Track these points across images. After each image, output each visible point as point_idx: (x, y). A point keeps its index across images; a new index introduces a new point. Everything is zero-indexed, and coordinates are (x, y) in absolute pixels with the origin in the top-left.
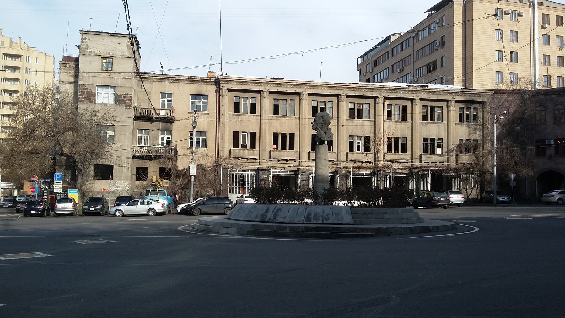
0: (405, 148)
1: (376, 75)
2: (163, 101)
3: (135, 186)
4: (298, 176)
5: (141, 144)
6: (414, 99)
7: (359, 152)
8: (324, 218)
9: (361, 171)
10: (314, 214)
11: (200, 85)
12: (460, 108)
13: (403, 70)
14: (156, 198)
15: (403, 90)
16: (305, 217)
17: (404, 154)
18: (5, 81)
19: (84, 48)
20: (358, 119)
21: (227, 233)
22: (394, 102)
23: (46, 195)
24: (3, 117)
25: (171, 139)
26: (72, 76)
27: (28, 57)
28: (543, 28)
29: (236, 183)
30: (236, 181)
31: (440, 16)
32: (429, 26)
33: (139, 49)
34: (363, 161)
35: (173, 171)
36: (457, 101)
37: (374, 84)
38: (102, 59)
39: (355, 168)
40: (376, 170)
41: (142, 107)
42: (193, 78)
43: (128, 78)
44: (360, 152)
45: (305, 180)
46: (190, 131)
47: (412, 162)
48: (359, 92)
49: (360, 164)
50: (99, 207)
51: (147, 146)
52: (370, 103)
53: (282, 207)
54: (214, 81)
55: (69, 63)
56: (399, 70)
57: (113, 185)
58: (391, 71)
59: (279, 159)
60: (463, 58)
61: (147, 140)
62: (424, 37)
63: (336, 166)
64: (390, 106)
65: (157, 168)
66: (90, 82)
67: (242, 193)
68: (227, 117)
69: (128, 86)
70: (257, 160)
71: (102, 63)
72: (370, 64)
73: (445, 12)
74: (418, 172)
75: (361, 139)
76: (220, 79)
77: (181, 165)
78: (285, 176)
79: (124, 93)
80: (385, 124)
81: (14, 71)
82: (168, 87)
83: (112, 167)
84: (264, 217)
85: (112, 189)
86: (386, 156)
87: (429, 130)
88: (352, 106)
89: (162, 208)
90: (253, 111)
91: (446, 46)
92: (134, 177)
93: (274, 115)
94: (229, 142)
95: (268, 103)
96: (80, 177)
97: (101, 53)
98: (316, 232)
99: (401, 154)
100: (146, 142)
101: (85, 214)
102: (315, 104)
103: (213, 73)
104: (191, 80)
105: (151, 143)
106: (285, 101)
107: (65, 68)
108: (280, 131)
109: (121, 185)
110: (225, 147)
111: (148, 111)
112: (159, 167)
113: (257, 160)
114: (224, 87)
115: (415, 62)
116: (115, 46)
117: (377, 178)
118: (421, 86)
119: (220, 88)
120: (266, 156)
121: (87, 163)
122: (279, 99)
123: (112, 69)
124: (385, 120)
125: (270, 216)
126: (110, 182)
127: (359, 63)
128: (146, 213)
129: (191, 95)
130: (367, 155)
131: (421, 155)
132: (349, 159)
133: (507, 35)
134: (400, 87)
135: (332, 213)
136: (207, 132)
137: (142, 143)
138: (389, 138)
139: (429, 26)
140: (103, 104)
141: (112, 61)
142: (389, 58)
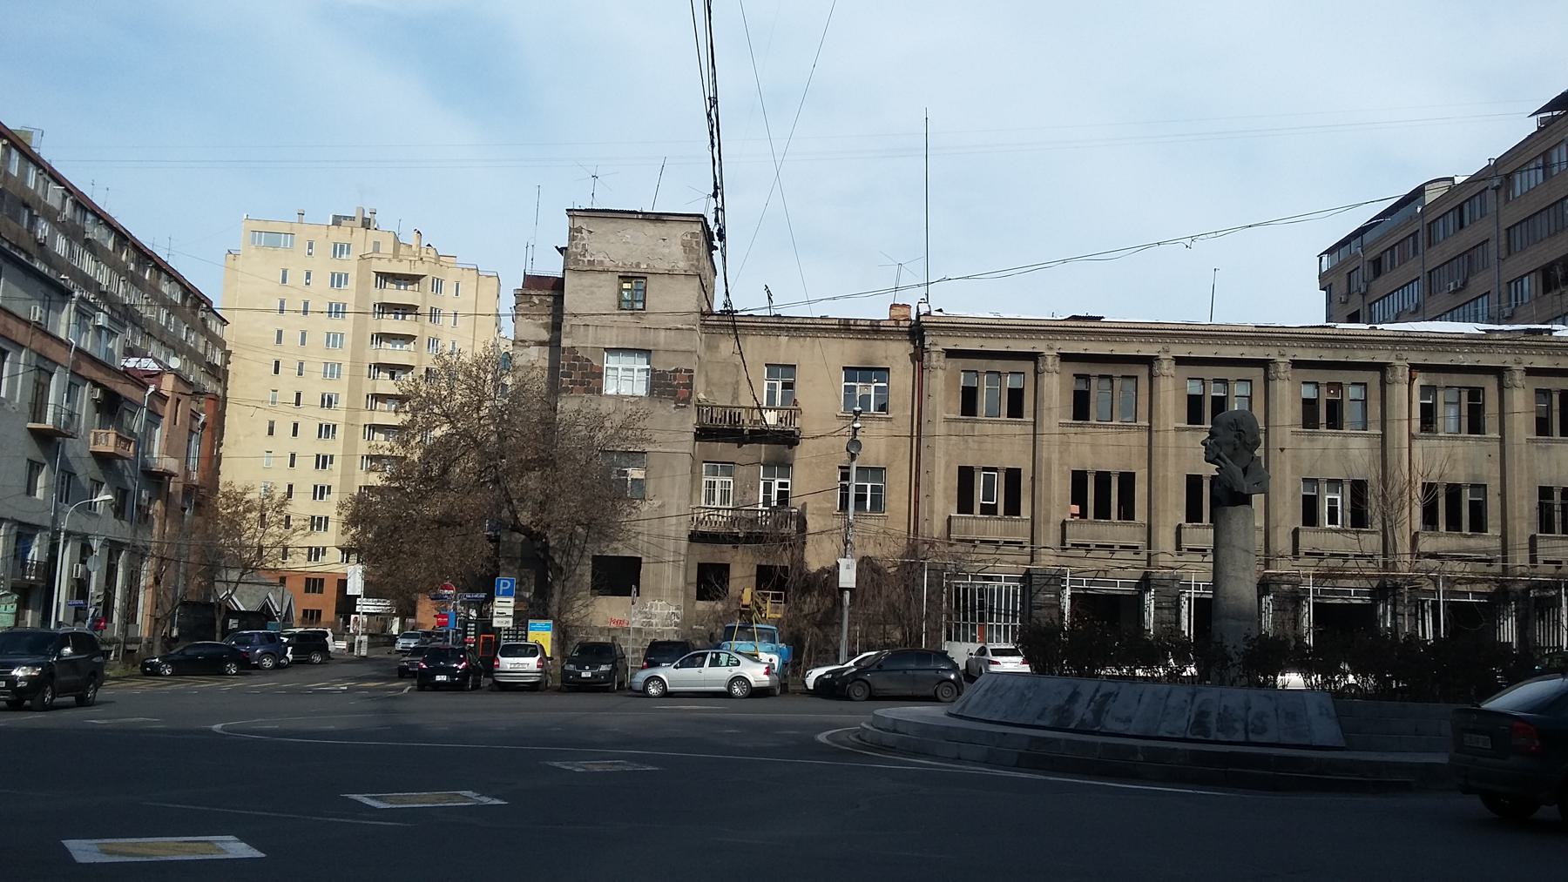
0: (1481, 517)
1: (1378, 300)
2: (772, 387)
3: (695, 615)
4: (1147, 596)
5: (712, 502)
6: (1508, 369)
8: (1250, 727)
9: (1343, 584)
10: (1219, 714)
13: (1465, 284)
14: (750, 649)
15: (1471, 342)
16: (1191, 721)
17: (1480, 536)
18: (381, 342)
19: (576, 254)
20: (1329, 431)
21: (959, 758)
22: (1441, 380)
23: (473, 633)
24: (373, 433)
26: (545, 326)
27: (438, 279)
29: (965, 612)
30: (965, 606)
32: (1546, 154)
33: (714, 252)
34: (1347, 555)
35: (792, 576)
37: (1379, 327)
38: (621, 281)
39: (1322, 576)
40: (1389, 583)
41: (718, 404)
42: (852, 322)
43: (683, 327)
44: (1339, 527)
45: (1169, 608)
46: (840, 467)
47: (1505, 560)
48: (1331, 352)
49: (1338, 562)
50: (603, 668)
51: (726, 507)
52: (1365, 384)
53: (1120, 688)
54: (907, 329)
55: (539, 292)
56: (1452, 284)
57: (639, 612)
58: (1427, 288)
59: (1088, 546)
61: (729, 491)
62: (1529, 186)
63: (1262, 568)
64: (1427, 390)
66: (590, 341)
67: (983, 640)
68: (941, 428)
69: (683, 348)
70: (1024, 547)
71: (621, 290)
72: (1360, 270)
74: (1526, 591)
76: (924, 324)
77: (815, 560)
78: (1106, 595)
79: (674, 368)
80: (1417, 444)
81: (404, 314)
82: (785, 349)
83: (635, 563)
84: (1065, 715)
85: (636, 622)
86: (1420, 542)
87: (1558, 464)
88: (1308, 392)
89: (767, 678)
90: (1015, 409)
92: (693, 591)
93: (1074, 422)
94: (947, 497)
95: (1056, 388)
96: (557, 590)
97: (617, 266)
98: (1230, 769)
99: (1469, 537)
100: (725, 496)
101: (568, 687)
102: (1195, 388)
103: (905, 309)
104: (846, 328)
105: (737, 499)
106: (1108, 381)
107: (527, 305)
110: (936, 509)
111: (732, 414)
112: (758, 563)
113: (1024, 547)
114: (936, 345)
115: (1503, 259)
116: (652, 247)
117: (1394, 605)
118: (1528, 331)
119: (923, 347)
120: (1050, 536)
121: (576, 553)
122: (1089, 375)
123: (644, 306)
124: (1413, 432)
125: (1084, 714)
126: (633, 604)
127: (1324, 269)
128: (723, 688)
129: (844, 368)
130: (1361, 536)
131: (1533, 539)
134: (1463, 336)
135: (1276, 711)
136: (885, 469)
137: (714, 500)
138: (1429, 488)
139: (1546, 154)
140: (618, 397)
141: (644, 284)
142: (1420, 251)
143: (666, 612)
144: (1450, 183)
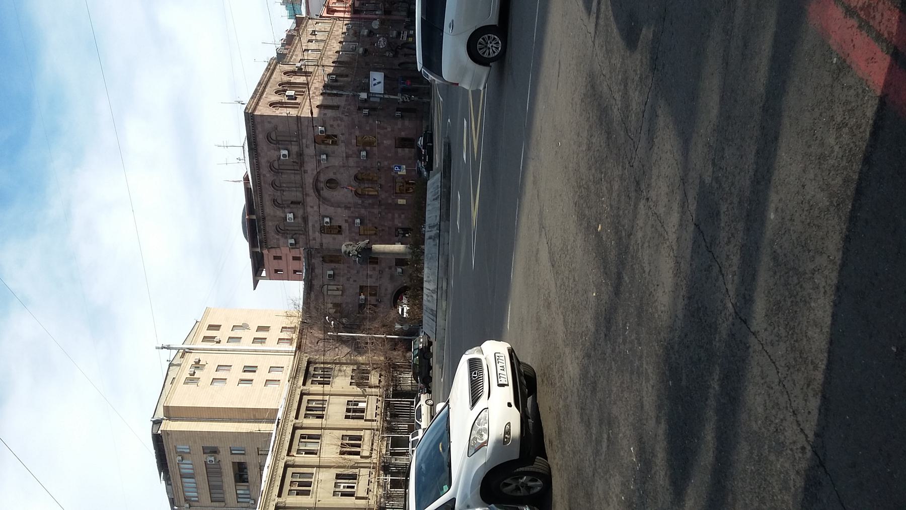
6: (294, 424)
7: (355, 487)
28: (219, 342)
32: (182, 476)
36: (304, 384)
44: (355, 485)
60: (239, 422)
64: (299, 451)
91: (218, 445)
115: (226, 504)
132: (365, 495)
133: (220, 375)
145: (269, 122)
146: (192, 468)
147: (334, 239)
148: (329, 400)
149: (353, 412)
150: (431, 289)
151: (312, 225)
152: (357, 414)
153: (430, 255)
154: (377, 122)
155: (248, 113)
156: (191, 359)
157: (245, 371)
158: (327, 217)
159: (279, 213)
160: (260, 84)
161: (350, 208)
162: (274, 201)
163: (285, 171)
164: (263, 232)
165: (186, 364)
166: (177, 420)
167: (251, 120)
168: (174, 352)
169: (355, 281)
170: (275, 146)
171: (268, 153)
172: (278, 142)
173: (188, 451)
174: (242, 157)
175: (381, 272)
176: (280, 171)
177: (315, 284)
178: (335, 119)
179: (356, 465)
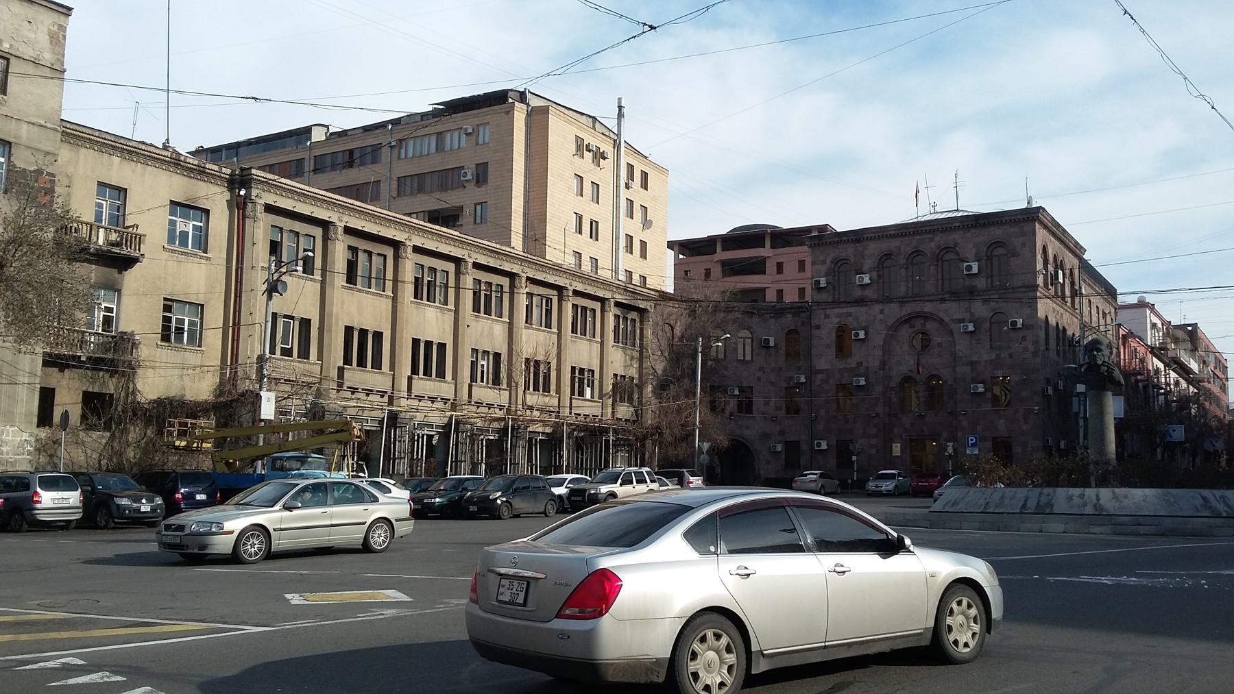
11: (193, 180)
12: (617, 317)
20: (485, 316)
25: (114, 315)
28: (627, 187)
31: (476, 121)
32: (440, 135)
36: (618, 304)
42: (182, 158)
43: (48, 125)
46: (165, 299)
54: (227, 177)
60: (525, 214)
65: (79, 394)
73: (489, 117)
75: (486, 357)
76: (255, 177)
82: (118, 171)
108: (357, 324)
109: (10, 438)
112: (84, 389)
116: (18, 27)
143: (19, 438)
144: (325, 130)
145: (1023, 245)
146: (453, 148)
147: (828, 346)
148: (596, 342)
149: (581, 379)
150: (1100, 502)
151: (851, 313)
152: (577, 385)
153: (1172, 500)
154: (1036, 408)
155: (1039, 212)
156: (607, 147)
157: (591, 223)
158: (866, 334)
159: (868, 263)
160: (1064, 231)
161: (884, 369)
162: (888, 255)
163: (940, 270)
164: (836, 239)
165: (601, 140)
166: (527, 126)
167: (1031, 217)
168: (612, 124)
169: (759, 379)
170: (984, 254)
171: (969, 245)
172: (990, 258)
173: (481, 141)
174: (938, 209)
175: (774, 419)
176: (940, 262)
177: (753, 320)
178: (1036, 342)
179: (513, 384)
